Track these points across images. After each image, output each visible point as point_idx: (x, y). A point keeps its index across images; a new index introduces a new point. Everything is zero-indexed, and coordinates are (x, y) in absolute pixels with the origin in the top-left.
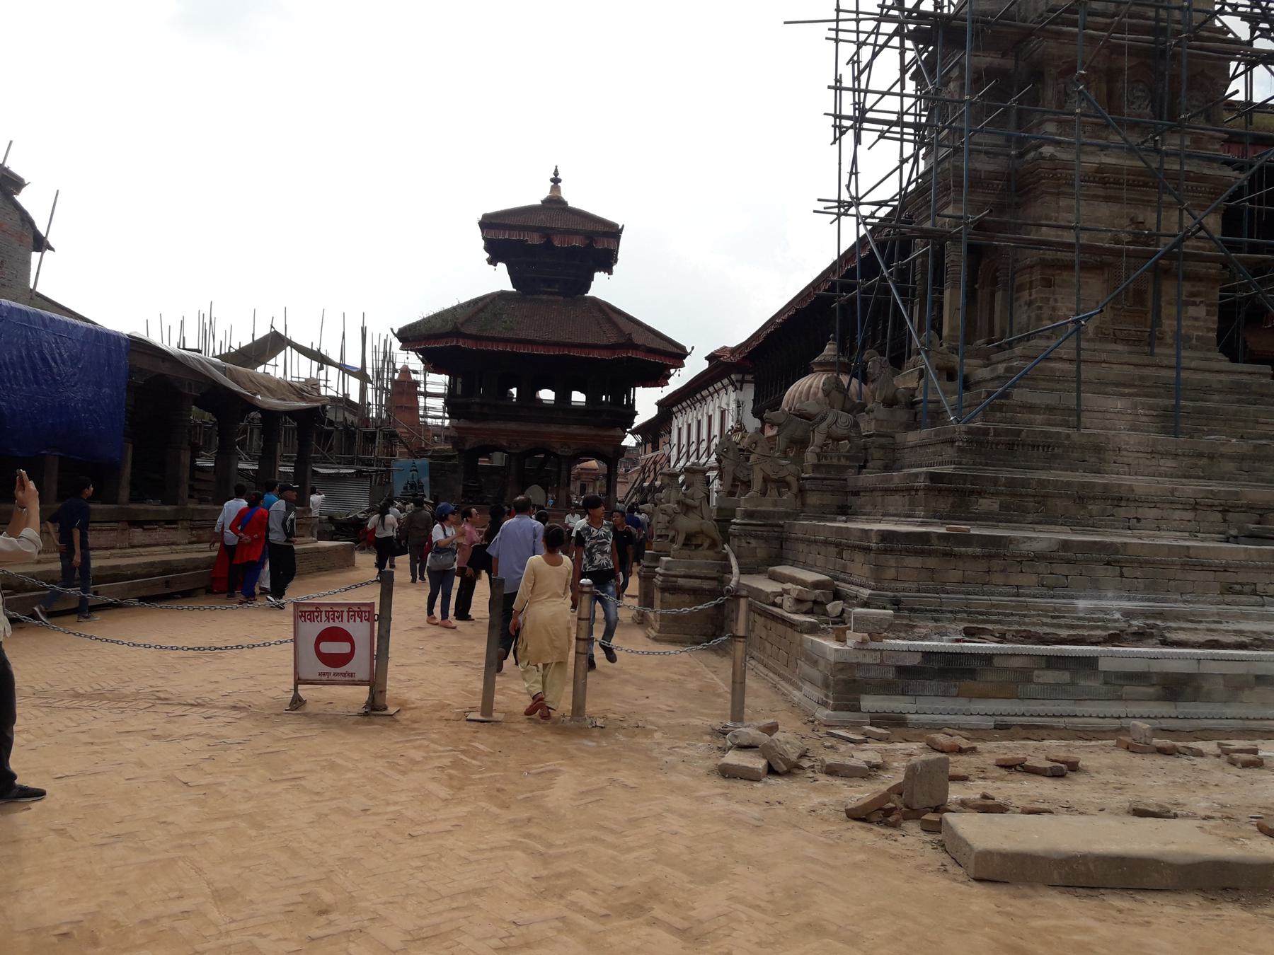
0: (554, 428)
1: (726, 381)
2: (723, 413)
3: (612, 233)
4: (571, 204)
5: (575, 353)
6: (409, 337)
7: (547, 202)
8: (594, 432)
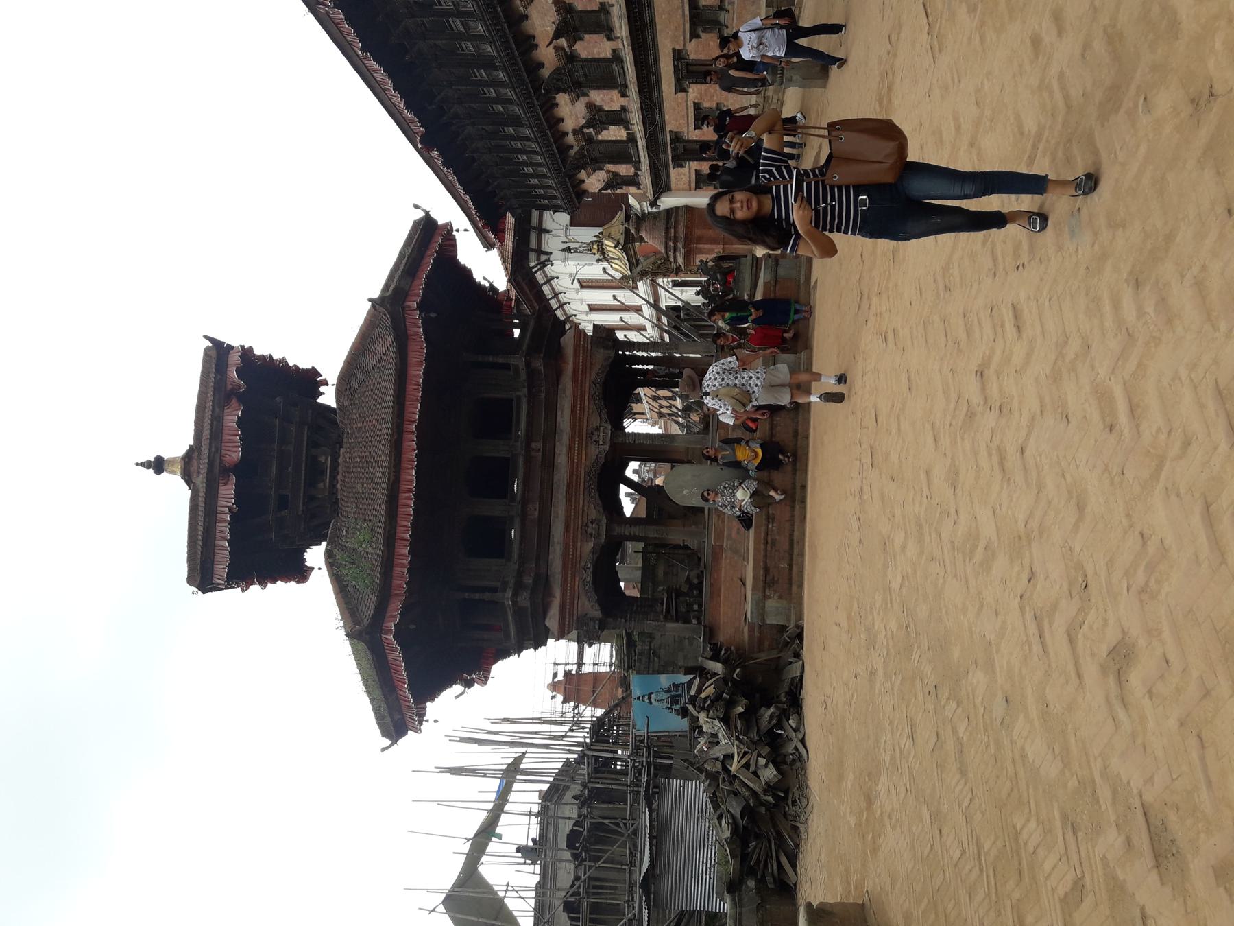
0: (562, 459)
1: (539, 277)
2: (585, 285)
3: (218, 353)
4: (189, 440)
5: (414, 411)
6: (397, 719)
7: (187, 477)
8: (567, 383)
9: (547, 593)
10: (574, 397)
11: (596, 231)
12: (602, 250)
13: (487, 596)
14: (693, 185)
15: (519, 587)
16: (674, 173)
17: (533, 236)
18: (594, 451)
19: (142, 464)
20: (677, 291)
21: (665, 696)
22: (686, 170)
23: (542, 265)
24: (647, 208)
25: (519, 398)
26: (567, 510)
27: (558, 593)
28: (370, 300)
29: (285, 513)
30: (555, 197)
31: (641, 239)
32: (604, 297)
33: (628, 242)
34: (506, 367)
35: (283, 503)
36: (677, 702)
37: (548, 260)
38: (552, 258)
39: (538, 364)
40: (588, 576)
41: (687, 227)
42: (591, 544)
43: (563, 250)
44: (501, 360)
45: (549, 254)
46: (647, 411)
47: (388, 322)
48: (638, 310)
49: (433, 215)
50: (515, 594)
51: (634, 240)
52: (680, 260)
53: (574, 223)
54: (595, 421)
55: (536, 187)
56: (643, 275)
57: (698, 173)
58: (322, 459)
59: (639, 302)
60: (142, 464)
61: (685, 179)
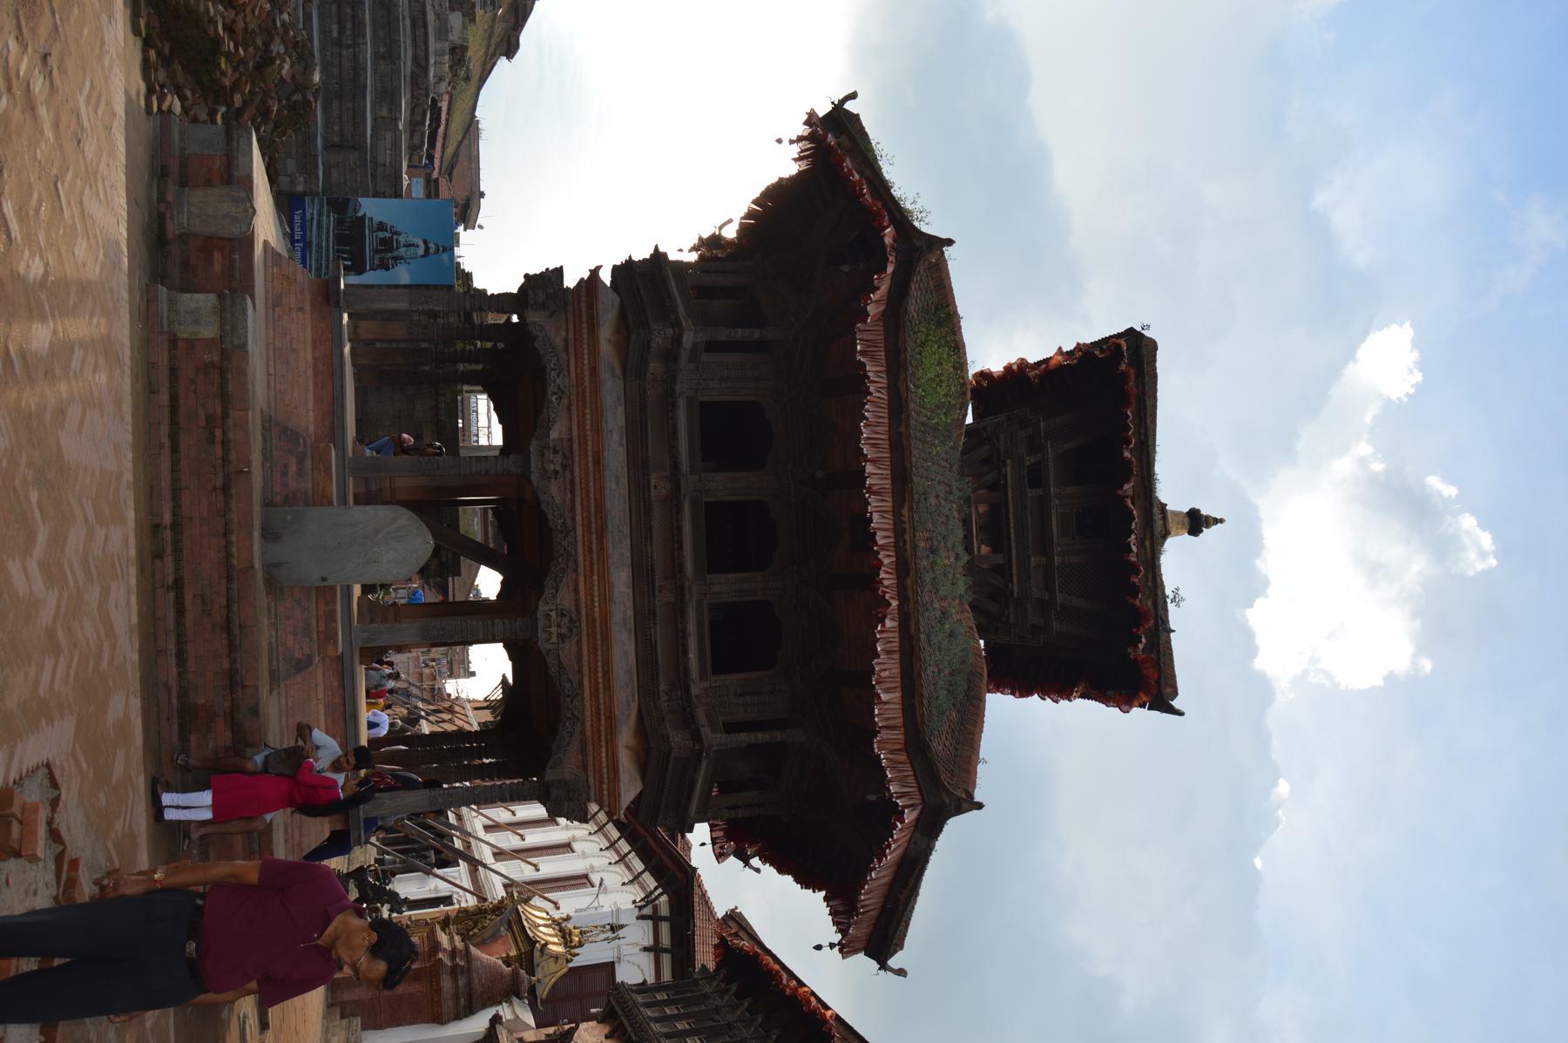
0: (621, 580)
1: (650, 882)
9: (622, 348)
10: (608, 687)
11: (577, 962)
12: (565, 935)
13: (724, 335)
15: (670, 355)
17: (666, 941)
18: (565, 599)
19: (1217, 521)
20: (444, 889)
21: (403, 250)
23: (648, 899)
24: (505, 1011)
25: (703, 677)
26: (601, 490)
27: (606, 348)
28: (980, 806)
29: (1029, 460)
30: (648, 1005)
31: (507, 961)
32: (551, 867)
33: (530, 952)
34: (730, 728)
35: (1036, 477)
36: (383, 241)
37: (640, 908)
38: (636, 912)
39: (677, 738)
40: (555, 381)
41: (438, 991)
42: (554, 435)
43: (622, 927)
44: (743, 738)
45: (642, 917)
46: (471, 713)
47: (944, 777)
48: (499, 854)
49: (874, 964)
50: (677, 340)
51: (519, 957)
52: (443, 939)
53: (609, 968)
54: (568, 650)
55: (678, 1018)
56: (499, 908)
58: (985, 549)
59: (500, 867)
60: (1217, 521)
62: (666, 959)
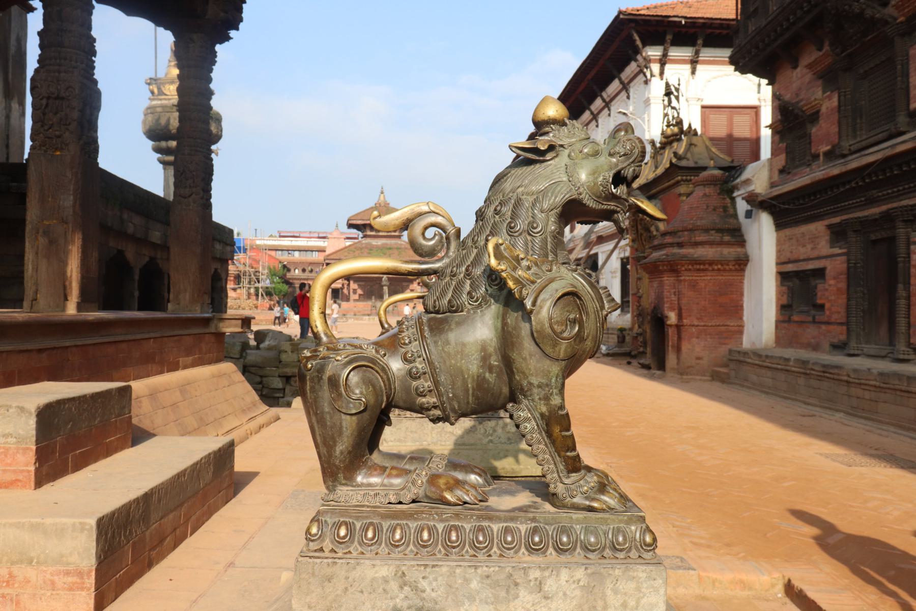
14: (790, 268)
16: (818, 228)
17: (686, 53)
22: (824, 248)
45: (662, 73)
57: (820, 273)
61: (804, 251)
62: (707, 53)
